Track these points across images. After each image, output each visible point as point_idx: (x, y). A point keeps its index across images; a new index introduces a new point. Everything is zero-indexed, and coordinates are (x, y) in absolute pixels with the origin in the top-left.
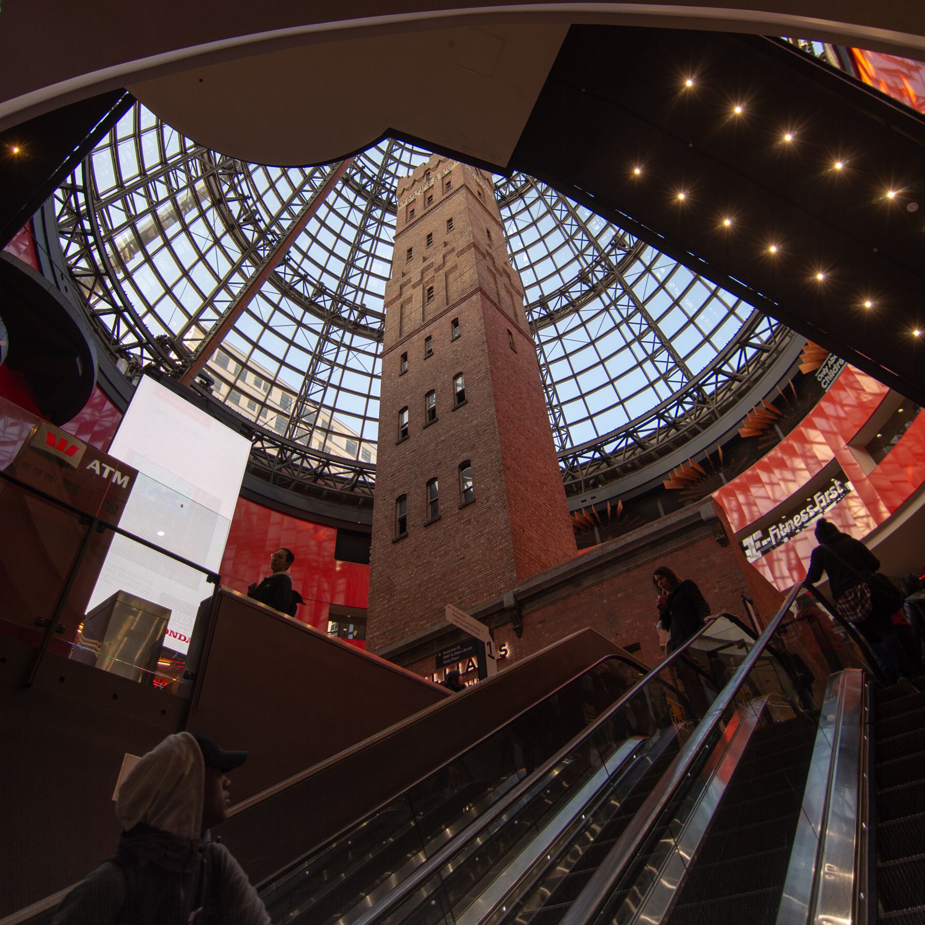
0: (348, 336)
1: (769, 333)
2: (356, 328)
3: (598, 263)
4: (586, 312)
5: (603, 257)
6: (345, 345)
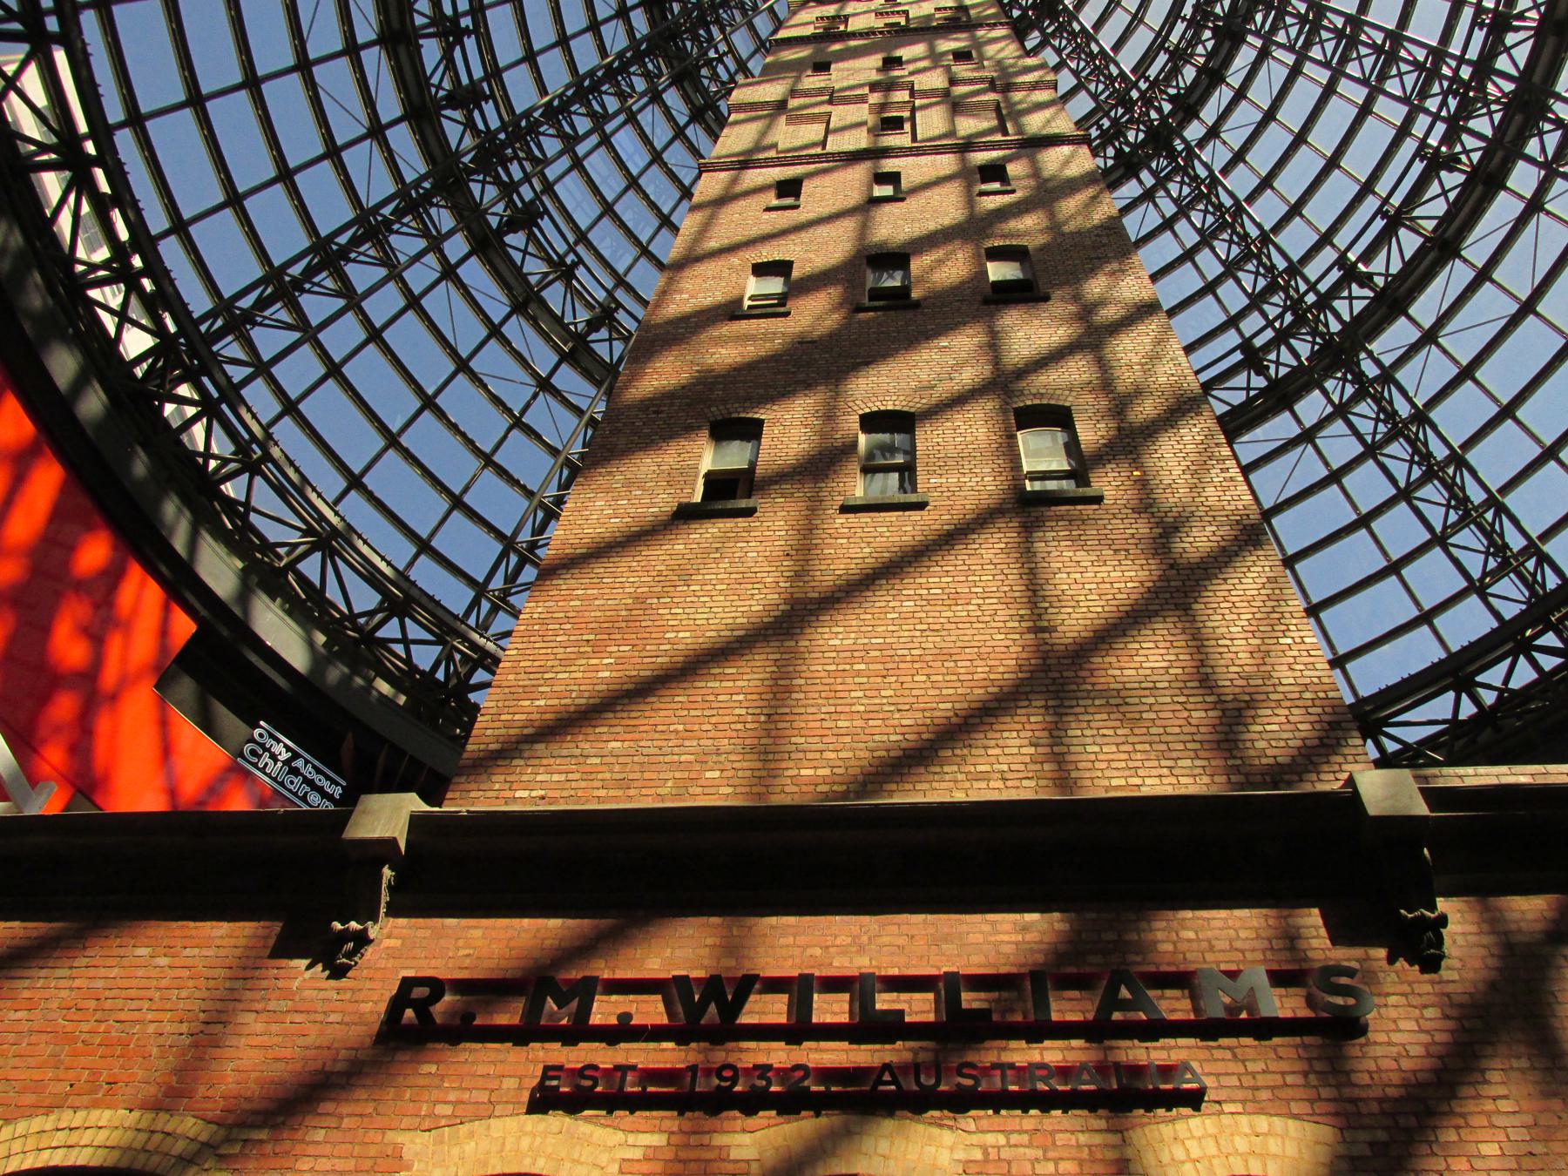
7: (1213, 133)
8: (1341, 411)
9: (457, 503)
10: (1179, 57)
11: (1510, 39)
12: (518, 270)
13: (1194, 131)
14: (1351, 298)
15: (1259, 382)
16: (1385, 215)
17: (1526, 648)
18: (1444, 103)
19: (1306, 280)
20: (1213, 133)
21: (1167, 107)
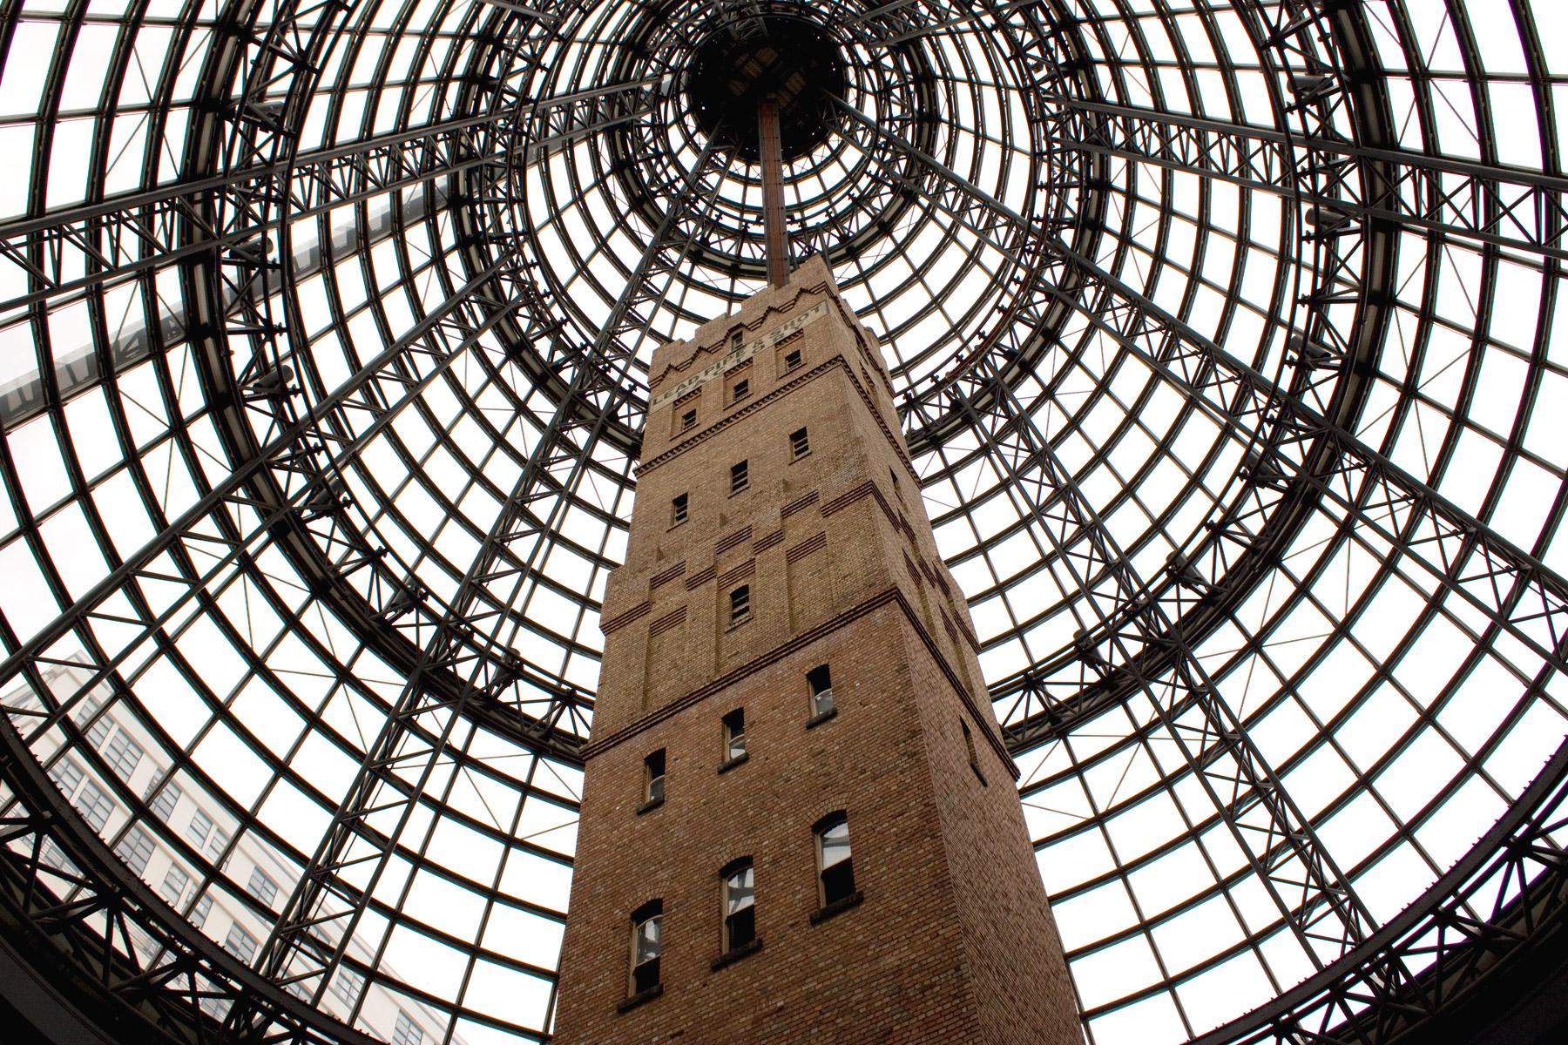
0: (463, 725)
2: (487, 712)
4: (1300, 556)
6: (450, 751)
7: (1049, 393)
8: (1167, 718)
10: (1009, 317)
11: (1317, 375)
12: (321, 557)
13: (1027, 391)
14: (1179, 600)
15: (1092, 676)
16: (1210, 526)
18: (1260, 427)
19: (1139, 581)
20: (1049, 393)
21: (1001, 362)
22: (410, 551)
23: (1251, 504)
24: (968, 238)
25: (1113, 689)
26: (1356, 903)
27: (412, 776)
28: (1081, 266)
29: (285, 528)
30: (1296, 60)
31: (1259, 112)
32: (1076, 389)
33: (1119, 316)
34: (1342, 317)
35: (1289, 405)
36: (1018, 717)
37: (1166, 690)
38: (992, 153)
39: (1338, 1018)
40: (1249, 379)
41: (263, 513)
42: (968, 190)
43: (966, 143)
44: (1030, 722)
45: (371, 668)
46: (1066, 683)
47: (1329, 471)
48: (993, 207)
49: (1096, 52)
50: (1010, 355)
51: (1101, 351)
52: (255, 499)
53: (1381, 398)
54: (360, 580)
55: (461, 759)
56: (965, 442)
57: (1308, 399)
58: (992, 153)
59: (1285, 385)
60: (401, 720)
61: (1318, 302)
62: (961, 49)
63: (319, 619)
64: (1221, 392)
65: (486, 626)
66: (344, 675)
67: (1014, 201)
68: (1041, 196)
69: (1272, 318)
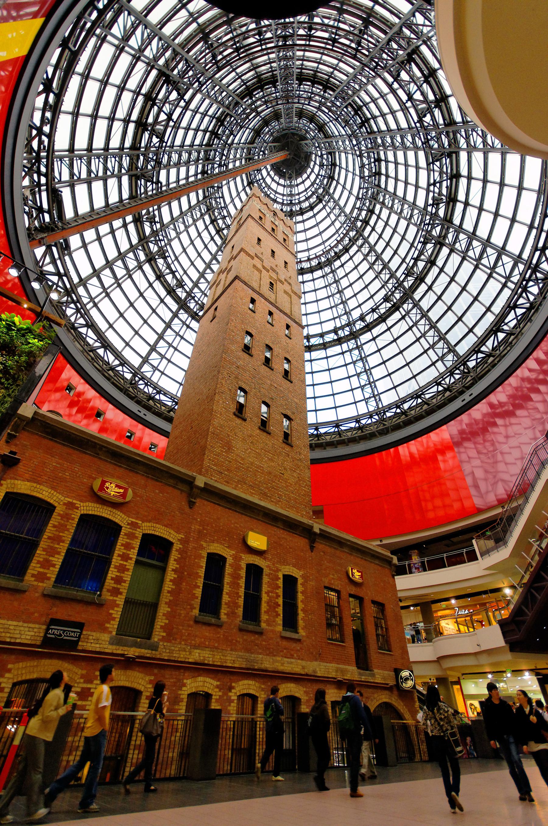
1: (515, 322)
3: (396, 288)
5: (400, 284)
8: (350, 351)
9: (137, 333)
11: (409, 278)
13: (337, 263)
15: (336, 337)
17: (371, 417)
22: (182, 272)
23: (383, 306)
24: (333, 217)
25: (339, 341)
26: (380, 400)
27: (177, 329)
28: (360, 233)
29: (151, 259)
30: (437, 190)
31: (421, 203)
32: (349, 266)
33: (365, 250)
34: (421, 265)
35: (400, 284)
36: (317, 343)
37: (352, 344)
38: (346, 193)
39: (370, 421)
40: (392, 275)
41: (146, 255)
42: (336, 203)
43: (340, 188)
44: (320, 344)
45: (169, 300)
46: (330, 337)
47: (404, 303)
48: (342, 210)
49: (383, 171)
50: (336, 253)
51: (359, 257)
52: (144, 250)
53: (423, 288)
54: (169, 278)
55: (188, 327)
56: (318, 273)
57: (405, 284)
58: (346, 193)
59: (401, 279)
60: (175, 315)
61: (416, 260)
62: (347, 158)
63: (157, 285)
64: (385, 276)
65: (199, 295)
66: (162, 301)
67: (348, 210)
68: (356, 210)
69: (404, 260)
